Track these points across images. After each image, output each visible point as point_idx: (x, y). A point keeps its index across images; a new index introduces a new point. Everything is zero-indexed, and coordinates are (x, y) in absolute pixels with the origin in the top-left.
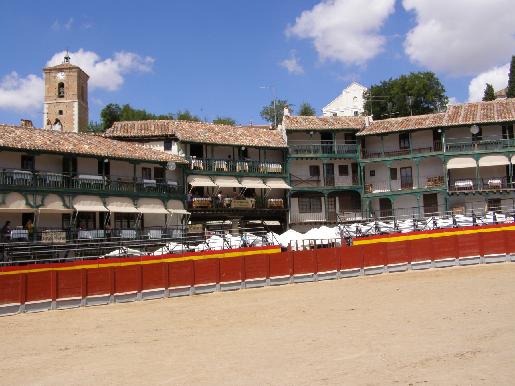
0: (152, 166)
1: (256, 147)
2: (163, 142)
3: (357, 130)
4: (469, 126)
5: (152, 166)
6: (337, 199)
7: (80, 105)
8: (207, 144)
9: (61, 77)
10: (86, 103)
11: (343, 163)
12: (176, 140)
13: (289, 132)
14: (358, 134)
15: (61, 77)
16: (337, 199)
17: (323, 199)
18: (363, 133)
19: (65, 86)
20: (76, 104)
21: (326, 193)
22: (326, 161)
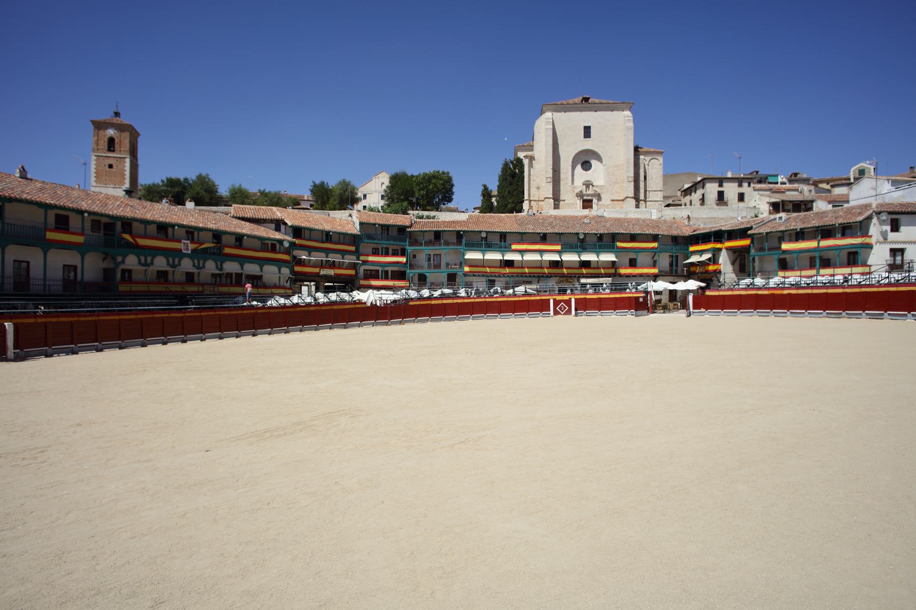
0: (269, 242)
1: (340, 234)
2: (273, 226)
4: (481, 232)
5: (269, 242)
7: (131, 161)
8: (305, 228)
9: (111, 132)
10: (137, 160)
11: (395, 247)
12: (285, 224)
13: (361, 224)
14: (409, 230)
15: (111, 132)
18: (412, 229)
19: (117, 141)
20: (128, 161)
22: (384, 246)
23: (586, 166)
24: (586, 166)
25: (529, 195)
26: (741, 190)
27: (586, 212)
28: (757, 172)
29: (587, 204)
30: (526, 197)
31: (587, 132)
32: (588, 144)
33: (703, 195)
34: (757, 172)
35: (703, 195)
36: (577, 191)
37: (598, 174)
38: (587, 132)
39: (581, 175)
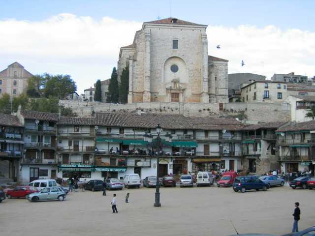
3: (56, 122)
6: (43, 153)
16: (43, 153)
17: (37, 153)
21: (40, 150)
23: (175, 69)
24: (175, 69)
25: (133, 88)
26: (279, 91)
27: (174, 105)
28: (293, 73)
29: (175, 96)
30: (130, 89)
31: (175, 43)
32: (177, 53)
33: (255, 94)
34: (293, 73)
35: (255, 94)
36: (168, 86)
37: (183, 75)
38: (175, 43)
39: (170, 76)
